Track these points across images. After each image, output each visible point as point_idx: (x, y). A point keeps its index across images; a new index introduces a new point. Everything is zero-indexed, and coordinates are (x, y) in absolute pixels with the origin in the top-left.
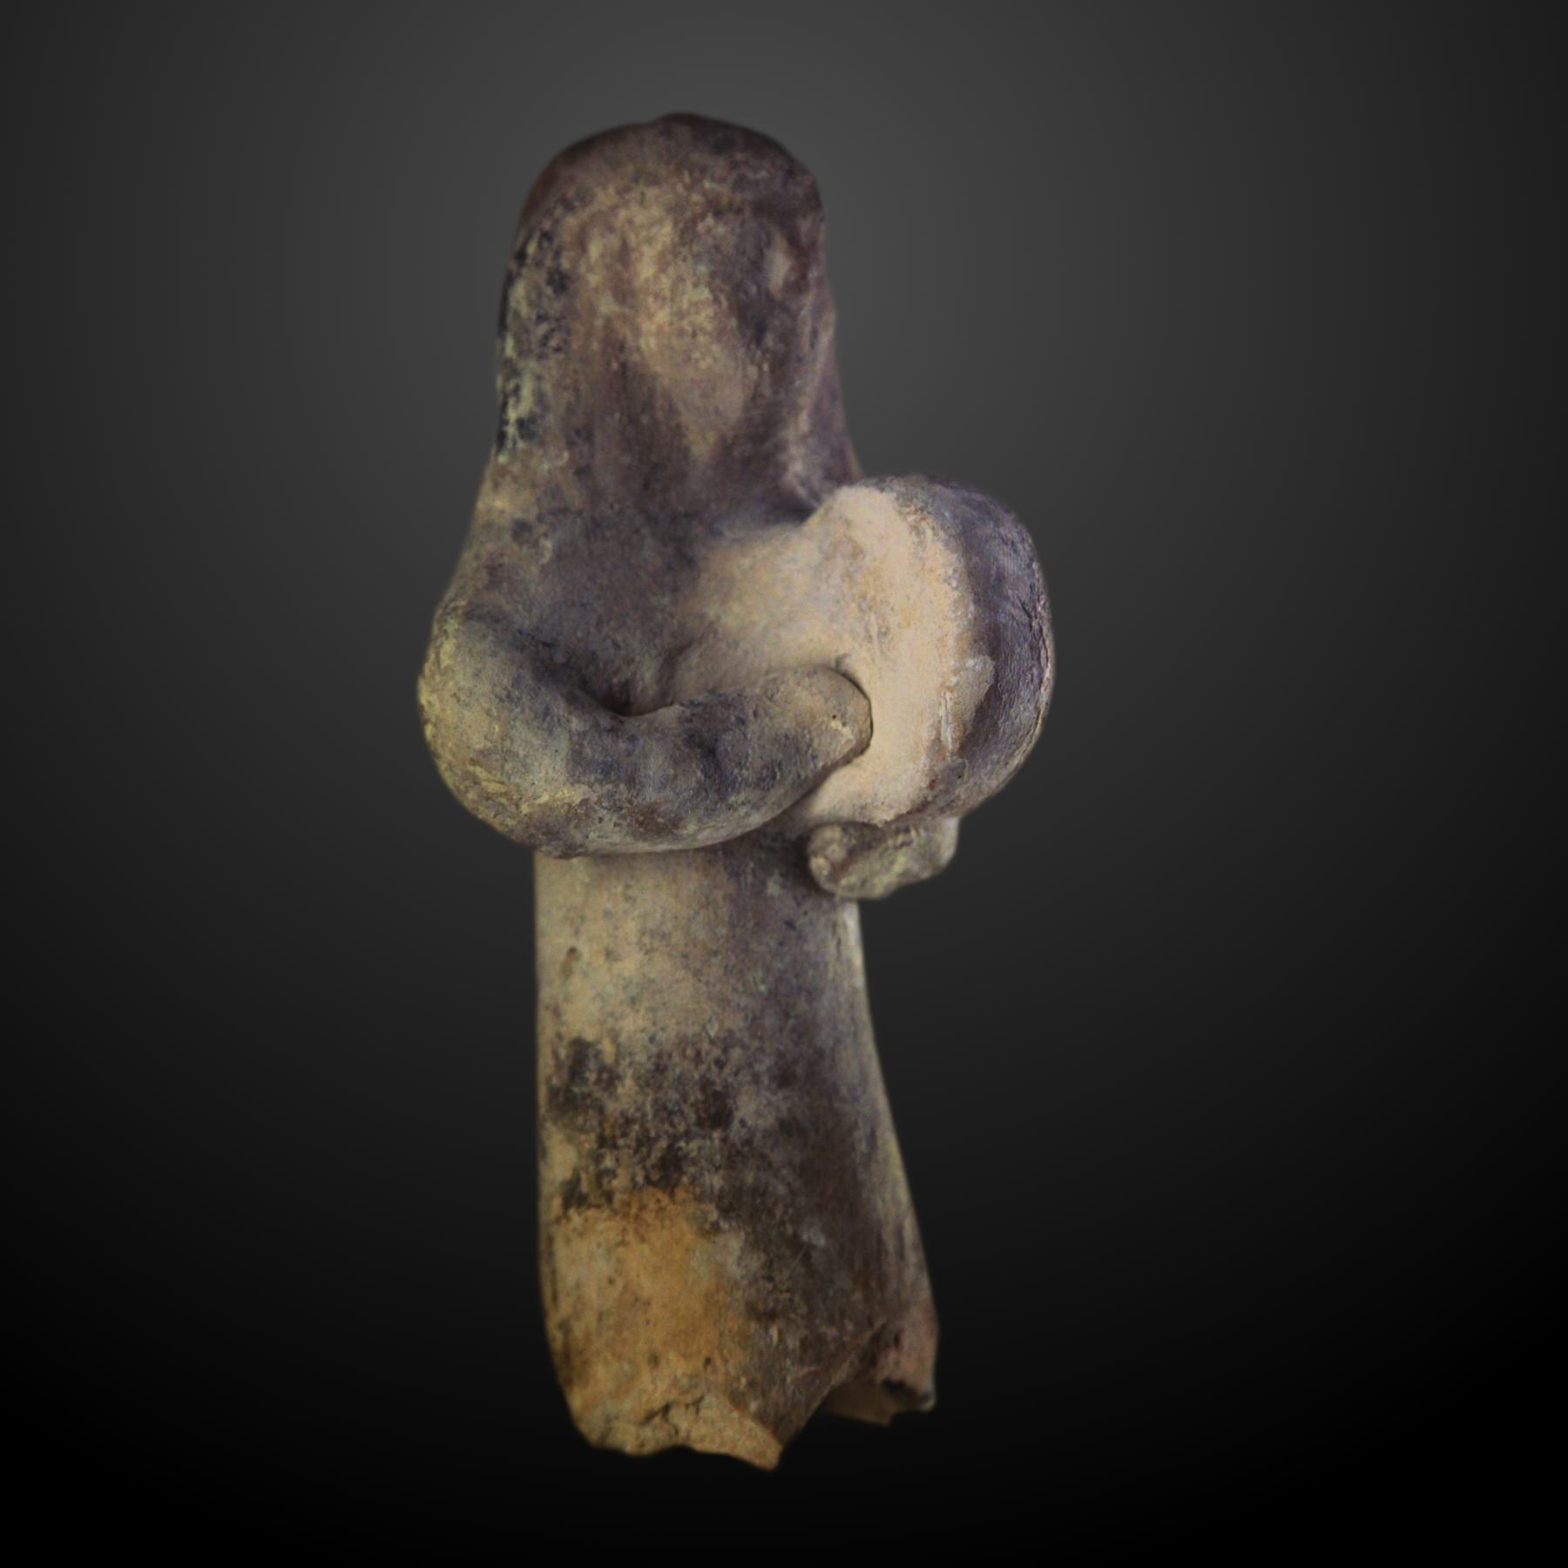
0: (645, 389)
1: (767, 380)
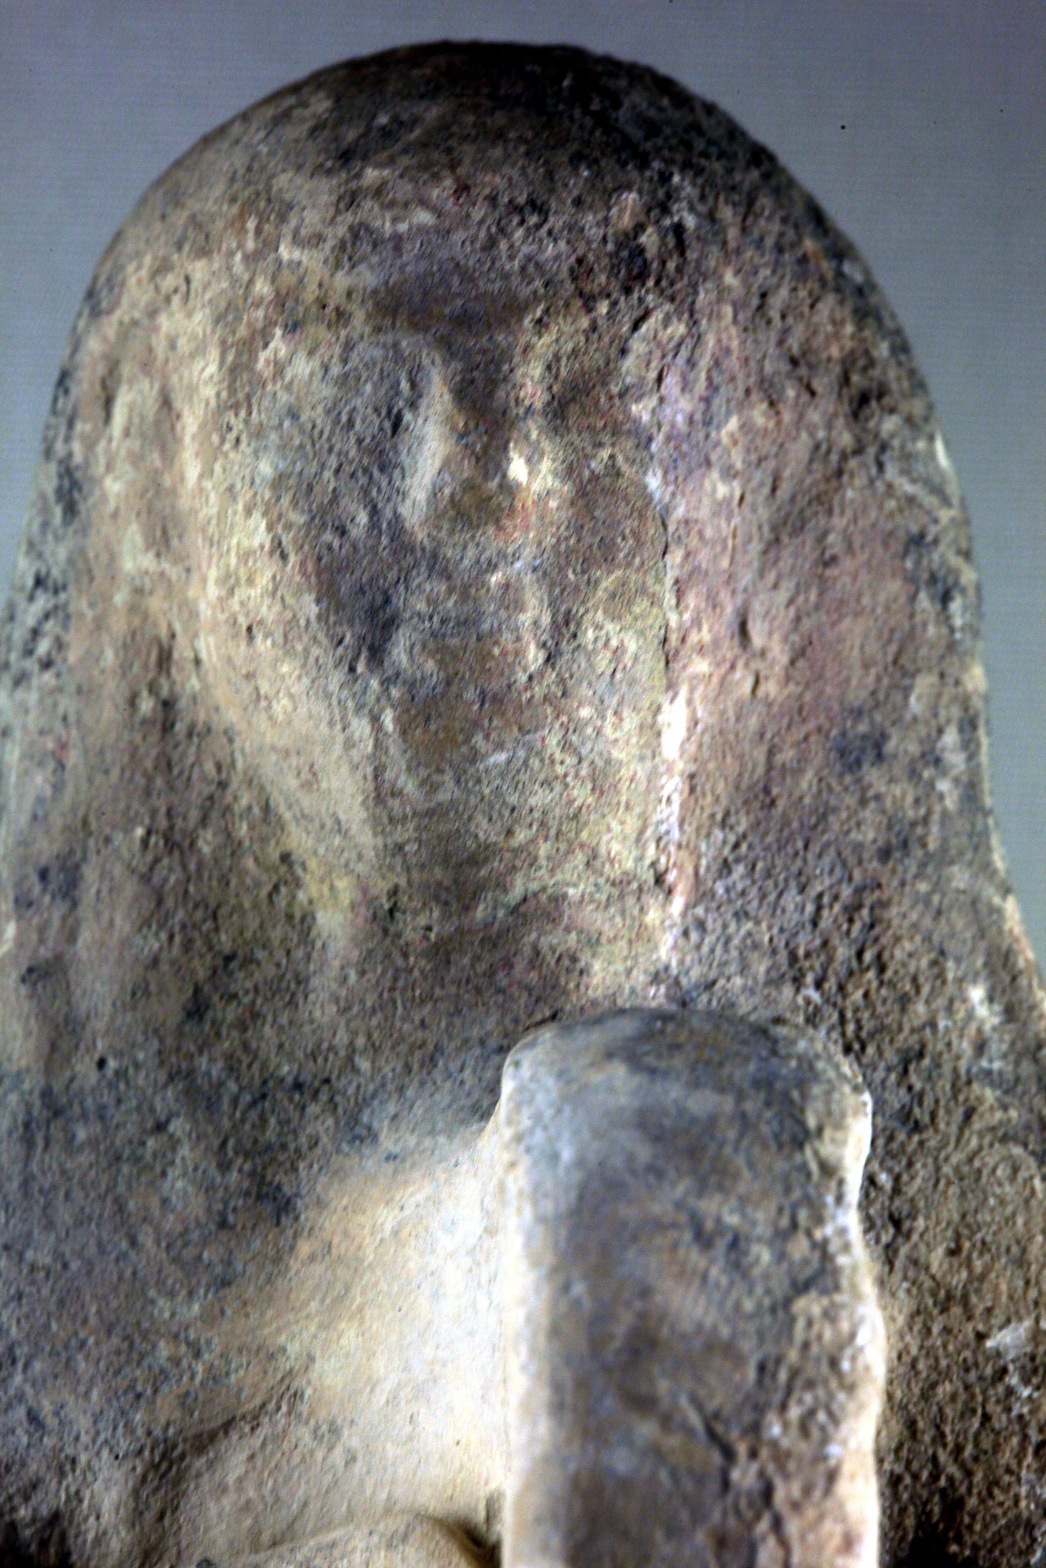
0: (209, 767)
1: (394, 747)
